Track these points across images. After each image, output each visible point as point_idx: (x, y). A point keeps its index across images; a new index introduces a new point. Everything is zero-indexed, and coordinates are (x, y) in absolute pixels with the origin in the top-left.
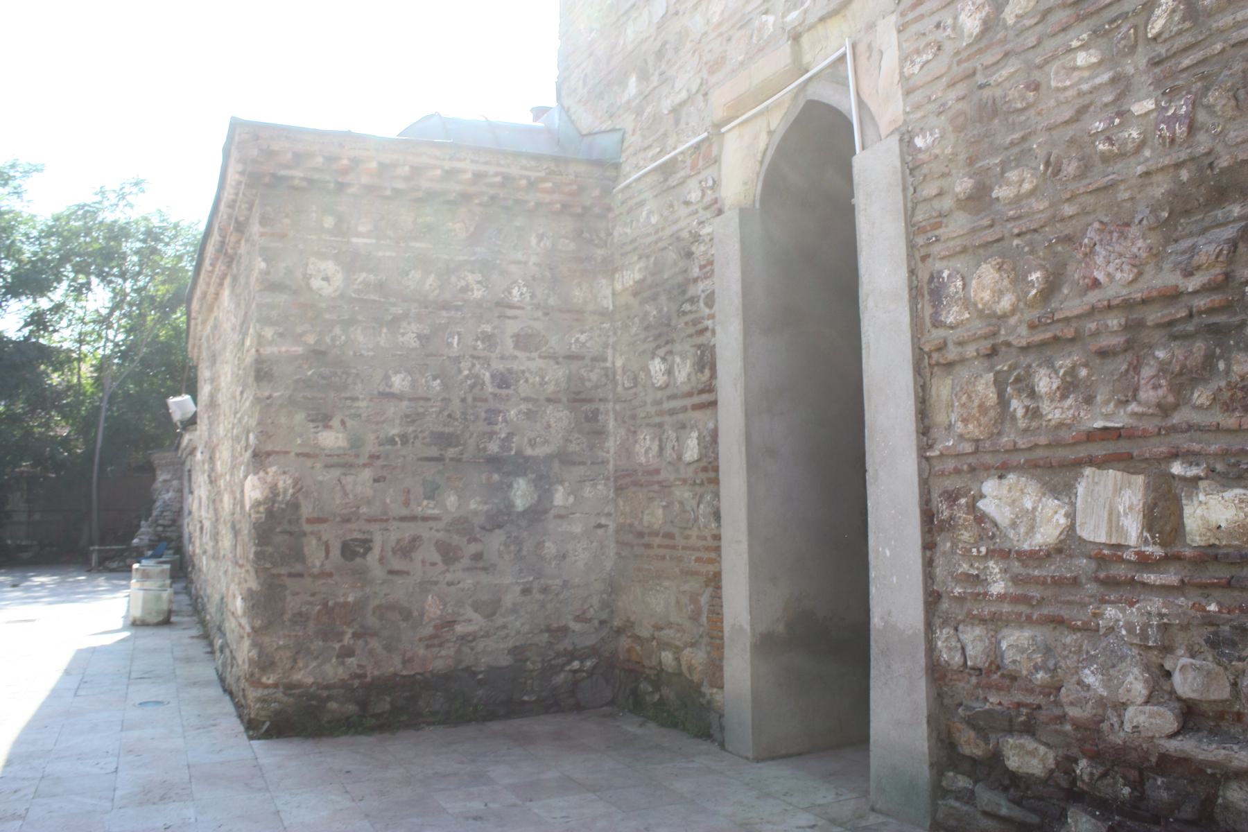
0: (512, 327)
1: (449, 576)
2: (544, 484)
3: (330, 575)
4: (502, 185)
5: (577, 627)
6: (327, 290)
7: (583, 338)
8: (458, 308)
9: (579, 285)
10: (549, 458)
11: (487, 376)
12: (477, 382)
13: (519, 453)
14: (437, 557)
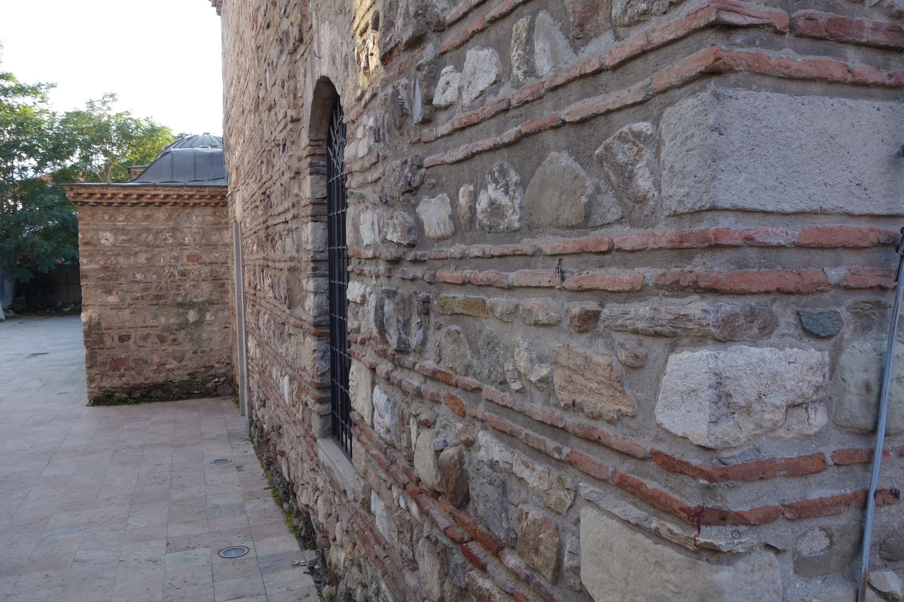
0: (186, 253)
1: (163, 348)
2: (202, 312)
3: (114, 348)
4: (177, 198)
5: (217, 365)
6: (107, 243)
7: (217, 255)
8: (162, 247)
9: (215, 234)
10: (204, 303)
11: (176, 273)
12: (172, 275)
13: (191, 301)
14: (157, 341)
